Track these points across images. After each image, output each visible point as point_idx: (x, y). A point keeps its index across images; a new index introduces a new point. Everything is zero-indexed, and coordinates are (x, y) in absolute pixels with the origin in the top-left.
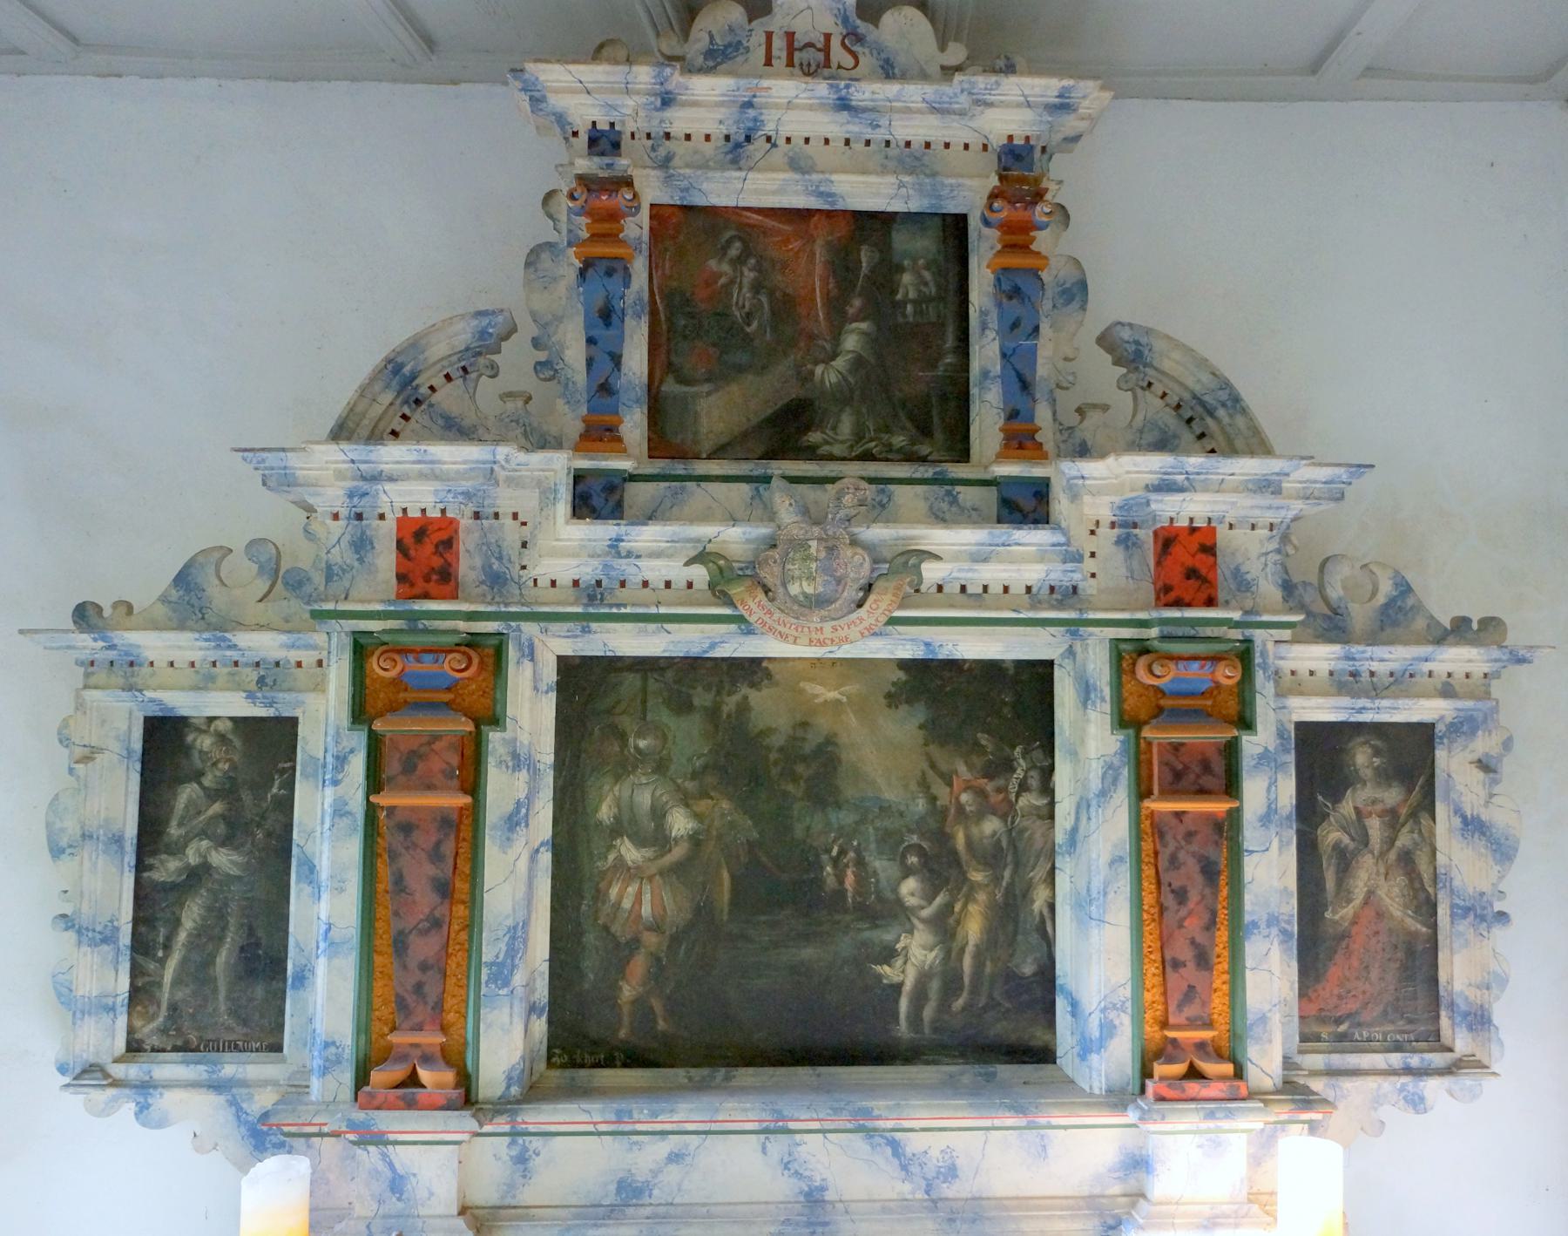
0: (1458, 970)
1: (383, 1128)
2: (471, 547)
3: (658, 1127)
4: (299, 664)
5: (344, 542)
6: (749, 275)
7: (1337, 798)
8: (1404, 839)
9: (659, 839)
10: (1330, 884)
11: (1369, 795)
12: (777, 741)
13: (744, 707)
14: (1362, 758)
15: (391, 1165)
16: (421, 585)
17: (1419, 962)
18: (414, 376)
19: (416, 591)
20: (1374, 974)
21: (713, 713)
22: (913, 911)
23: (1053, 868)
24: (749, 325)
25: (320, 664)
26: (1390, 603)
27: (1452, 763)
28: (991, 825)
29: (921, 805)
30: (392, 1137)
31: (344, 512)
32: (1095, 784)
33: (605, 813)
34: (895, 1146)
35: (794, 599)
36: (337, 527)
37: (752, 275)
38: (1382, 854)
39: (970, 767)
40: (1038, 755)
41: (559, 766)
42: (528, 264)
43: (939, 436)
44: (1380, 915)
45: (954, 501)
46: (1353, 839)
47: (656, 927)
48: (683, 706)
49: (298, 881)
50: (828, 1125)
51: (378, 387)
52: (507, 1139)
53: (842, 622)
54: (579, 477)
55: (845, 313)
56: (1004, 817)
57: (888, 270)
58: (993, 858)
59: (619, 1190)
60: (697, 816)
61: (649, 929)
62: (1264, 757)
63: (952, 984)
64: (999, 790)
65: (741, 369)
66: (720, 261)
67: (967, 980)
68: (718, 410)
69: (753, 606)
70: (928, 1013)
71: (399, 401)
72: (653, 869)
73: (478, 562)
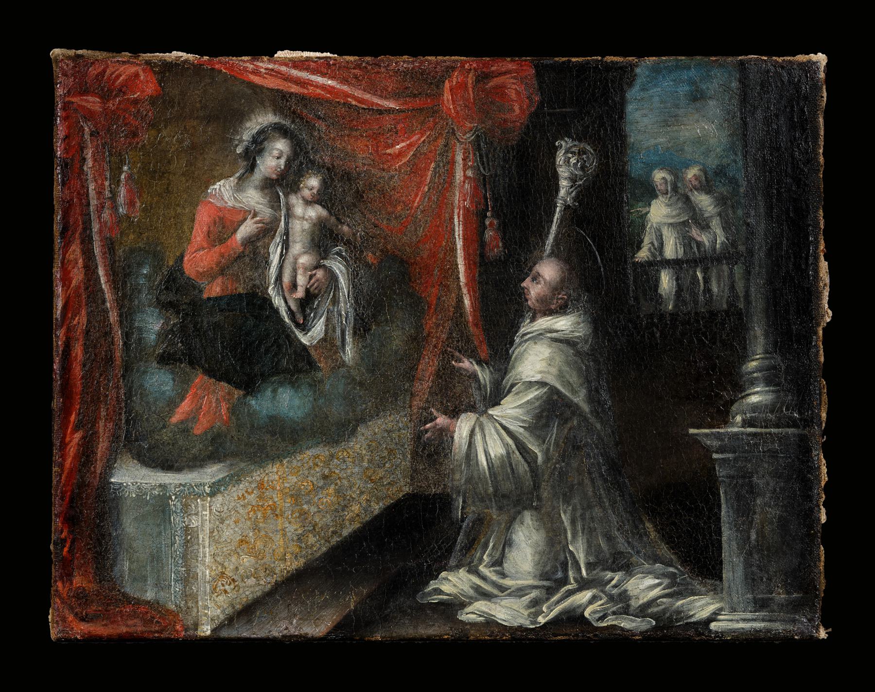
6: (305, 214)
24: (305, 328)
37: (315, 212)
55: (521, 295)
66: (240, 186)
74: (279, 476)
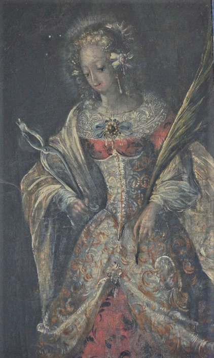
10: (44, 274)
38: (131, 217)
44: (129, 324)
46: (80, 195)
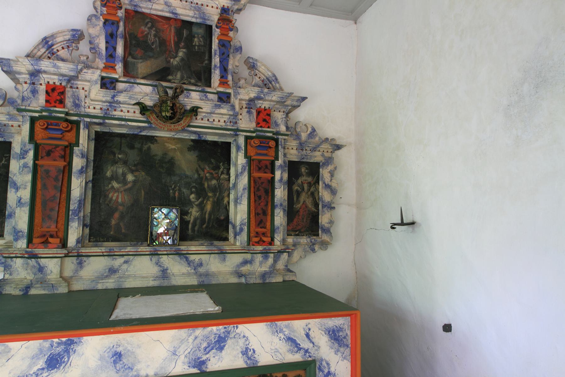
0: (324, 219)
1: (37, 252)
2: (69, 96)
3: (121, 253)
4: (12, 126)
5: (28, 91)
6: (153, 33)
7: (297, 179)
8: (312, 189)
9: (124, 181)
10: (295, 199)
11: (305, 179)
12: (158, 158)
13: (149, 149)
14: (303, 170)
15: (39, 264)
16: (53, 104)
17: (314, 218)
18: (52, 45)
19: (52, 105)
20: (305, 220)
21: (140, 150)
22: (194, 202)
23: (229, 193)
25: (19, 126)
26: (311, 133)
27: (325, 173)
28: (214, 182)
29: (196, 176)
30: (40, 256)
31: (28, 82)
32: (240, 170)
33: (109, 174)
34: (187, 259)
35: (164, 117)
36: (26, 86)
38: (307, 193)
39: (209, 167)
40: (226, 165)
41: (94, 161)
42: (88, 20)
43: (203, 80)
44: (306, 207)
45: (206, 97)
47: (122, 204)
48: (132, 147)
49: (11, 188)
50: (169, 252)
51: (40, 46)
52: (76, 258)
53: (176, 124)
54: (103, 78)
56: (217, 180)
57: (191, 37)
58: (214, 190)
59: (109, 271)
60: (135, 176)
61: (121, 205)
62: (281, 166)
63: (203, 221)
64: (216, 173)
65: (150, 57)
66: (145, 27)
67: (207, 220)
68: (143, 67)
69: (152, 118)
70: (196, 228)
71: (47, 52)
72: (122, 189)
73: (71, 100)
74: (149, 63)
